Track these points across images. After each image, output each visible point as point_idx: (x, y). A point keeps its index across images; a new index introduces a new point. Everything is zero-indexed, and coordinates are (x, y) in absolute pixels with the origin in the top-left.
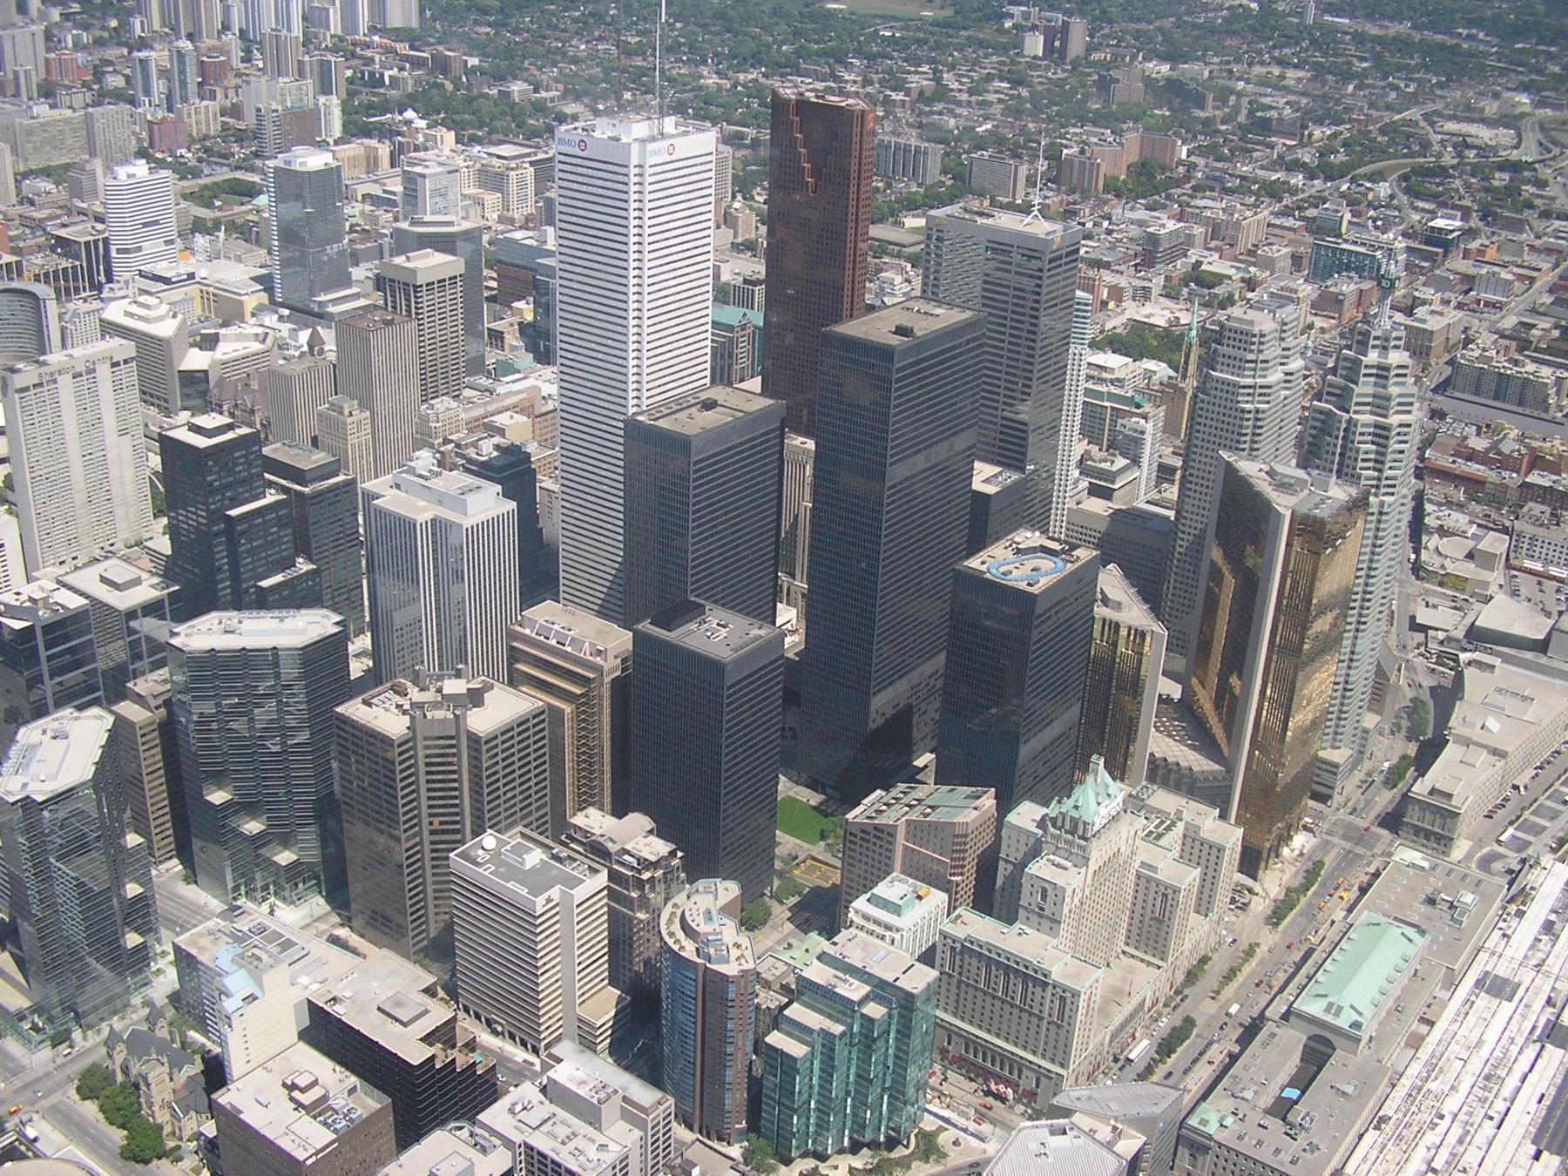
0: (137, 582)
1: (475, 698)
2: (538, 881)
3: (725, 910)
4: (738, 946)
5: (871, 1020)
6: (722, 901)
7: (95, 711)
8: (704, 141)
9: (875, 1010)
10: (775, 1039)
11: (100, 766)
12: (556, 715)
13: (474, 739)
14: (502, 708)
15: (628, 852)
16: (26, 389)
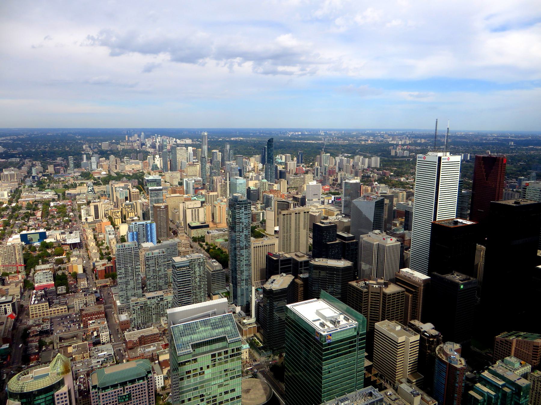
0: (303, 256)
1: (386, 285)
2: (399, 334)
3: (456, 351)
4: (461, 361)
5: (506, 392)
6: (455, 349)
7: (290, 275)
8: (458, 158)
9: (506, 389)
10: (472, 393)
11: (290, 286)
12: (408, 297)
13: (385, 294)
14: (392, 289)
15: (426, 332)
16: (284, 215)
